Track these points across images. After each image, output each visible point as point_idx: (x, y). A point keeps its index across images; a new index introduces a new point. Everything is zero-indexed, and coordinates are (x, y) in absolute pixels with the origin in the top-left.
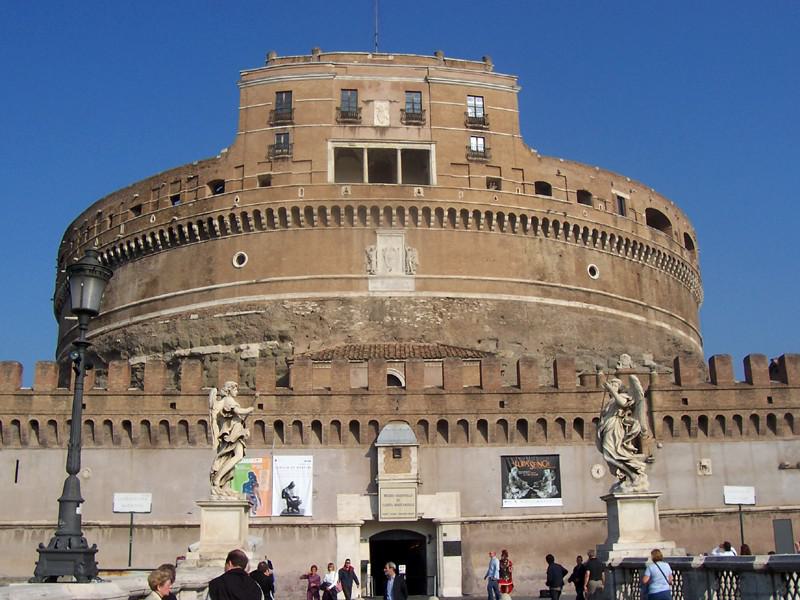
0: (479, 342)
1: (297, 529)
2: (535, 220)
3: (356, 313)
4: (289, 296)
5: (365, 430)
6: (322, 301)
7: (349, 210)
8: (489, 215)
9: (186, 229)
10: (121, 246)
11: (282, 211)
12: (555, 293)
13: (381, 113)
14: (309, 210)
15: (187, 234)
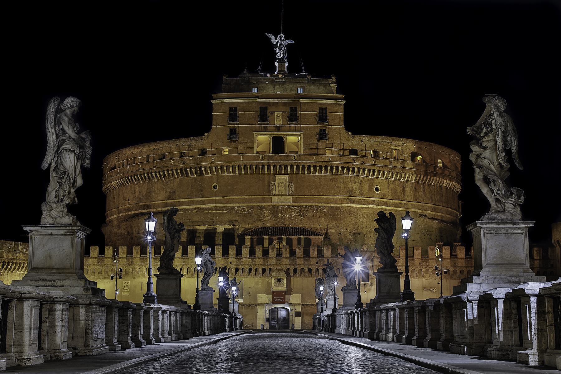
0: (320, 225)
1: (243, 307)
2: (348, 168)
3: (267, 213)
4: (237, 205)
5: (267, 272)
6: (252, 207)
7: (263, 166)
8: (326, 168)
9: (188, 170)
10: (155, 173)
11: (233, 167)
12: (357, 201)
13: (278, 118)
14: (245, 167)
15: (189, 173)
